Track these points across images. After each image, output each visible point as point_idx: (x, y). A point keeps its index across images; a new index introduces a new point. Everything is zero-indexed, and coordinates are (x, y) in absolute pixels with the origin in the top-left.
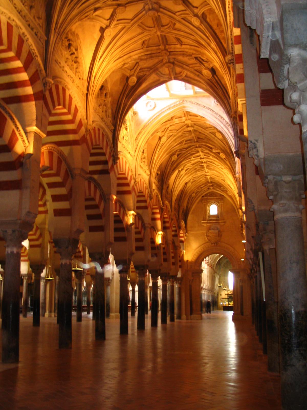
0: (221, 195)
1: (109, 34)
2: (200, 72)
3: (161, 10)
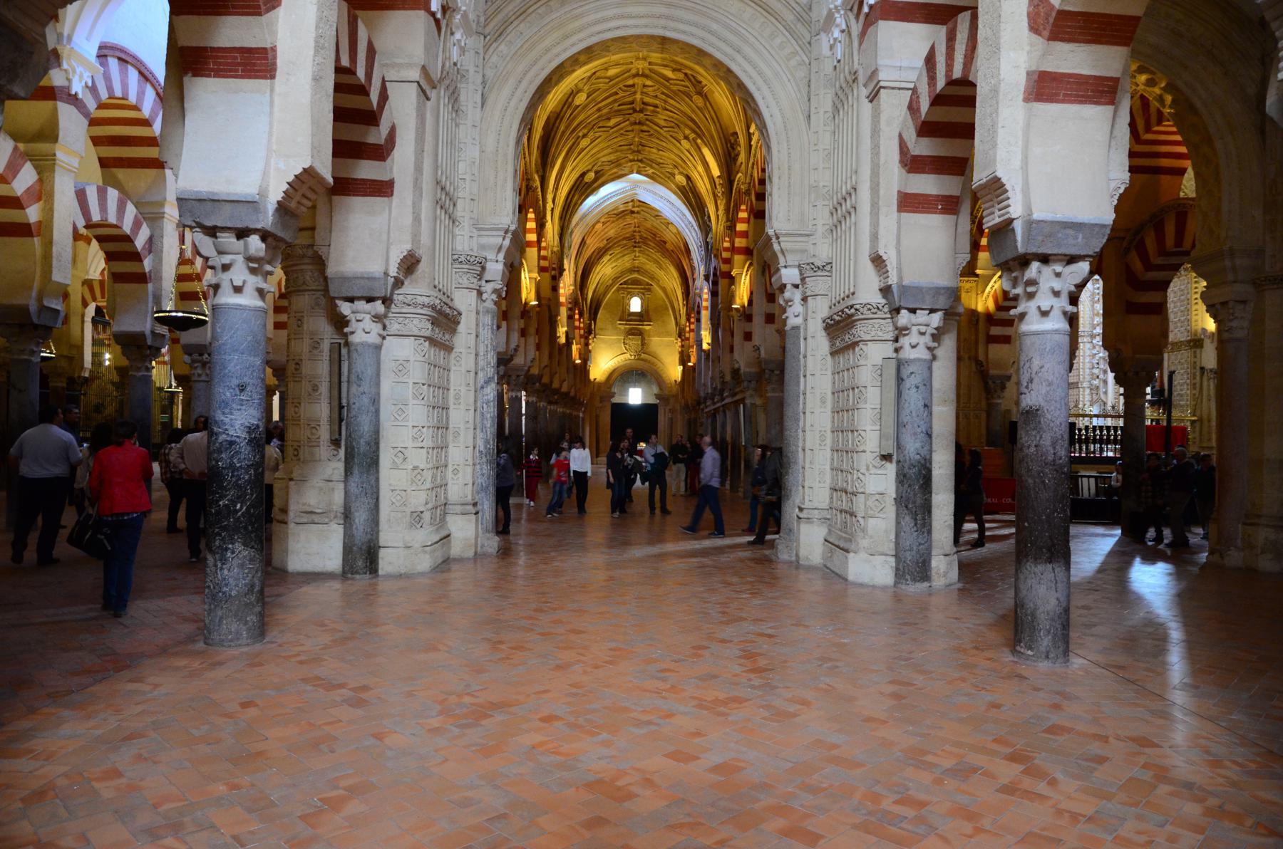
0: (648, 284)
1: (584, 142)
2: (673, 175)
3: (648, 122)
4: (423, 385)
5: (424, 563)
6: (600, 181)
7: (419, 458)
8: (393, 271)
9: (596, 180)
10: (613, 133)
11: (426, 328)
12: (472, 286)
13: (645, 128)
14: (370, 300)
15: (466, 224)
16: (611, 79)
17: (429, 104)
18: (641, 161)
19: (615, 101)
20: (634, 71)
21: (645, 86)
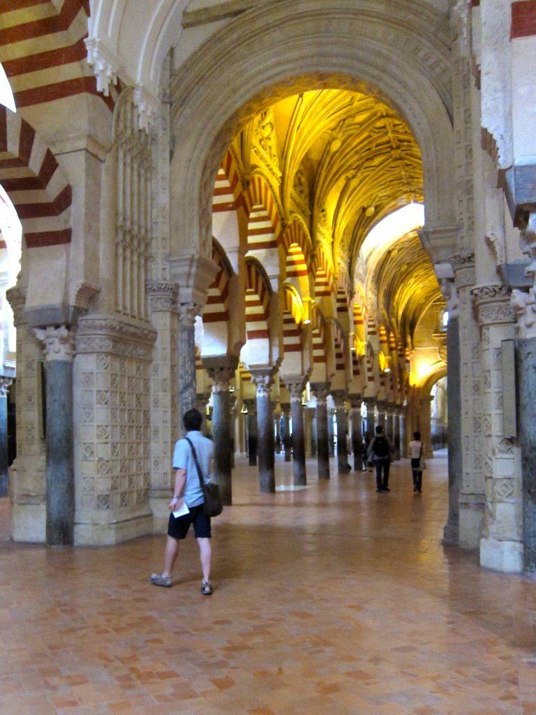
4: (106, 392)
5: (110, 538)
6: (381, 214)
7: (103, 451)
8: (72, 301)
9: (376, 213)
10: (379, 171)
11: (108, 345)
12: (165, 309)
13: (409, 163)
14: (57, 327)
15: (159, 259)
16: (361, 124)
17: (103, 166)
18: (414, 192)
19: (370, 143)
20: (379, 114)
21: (395, 125)
